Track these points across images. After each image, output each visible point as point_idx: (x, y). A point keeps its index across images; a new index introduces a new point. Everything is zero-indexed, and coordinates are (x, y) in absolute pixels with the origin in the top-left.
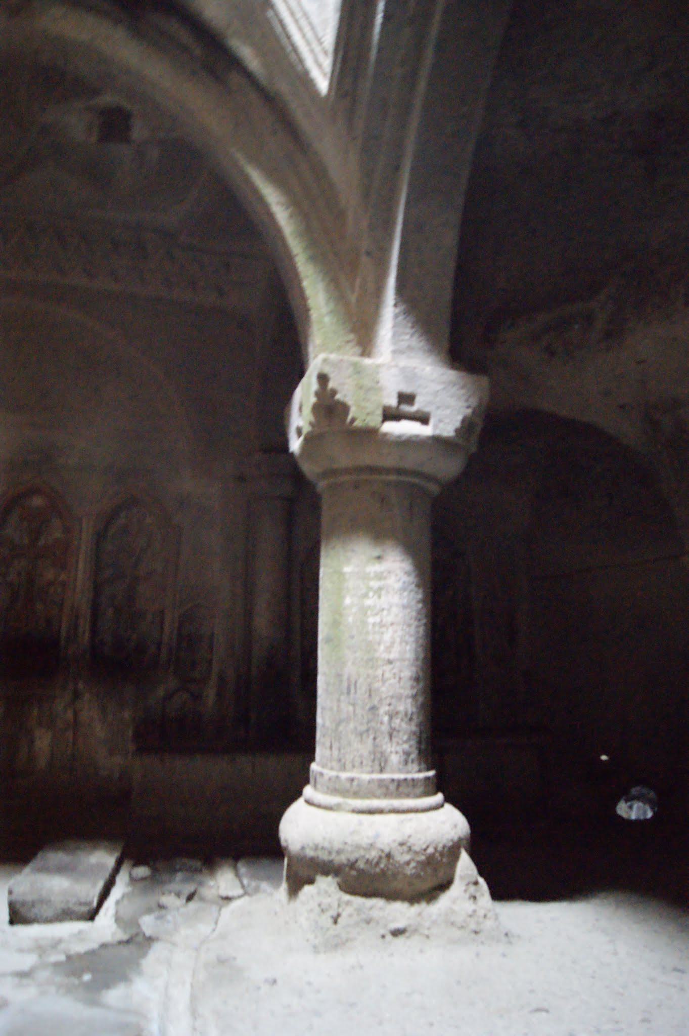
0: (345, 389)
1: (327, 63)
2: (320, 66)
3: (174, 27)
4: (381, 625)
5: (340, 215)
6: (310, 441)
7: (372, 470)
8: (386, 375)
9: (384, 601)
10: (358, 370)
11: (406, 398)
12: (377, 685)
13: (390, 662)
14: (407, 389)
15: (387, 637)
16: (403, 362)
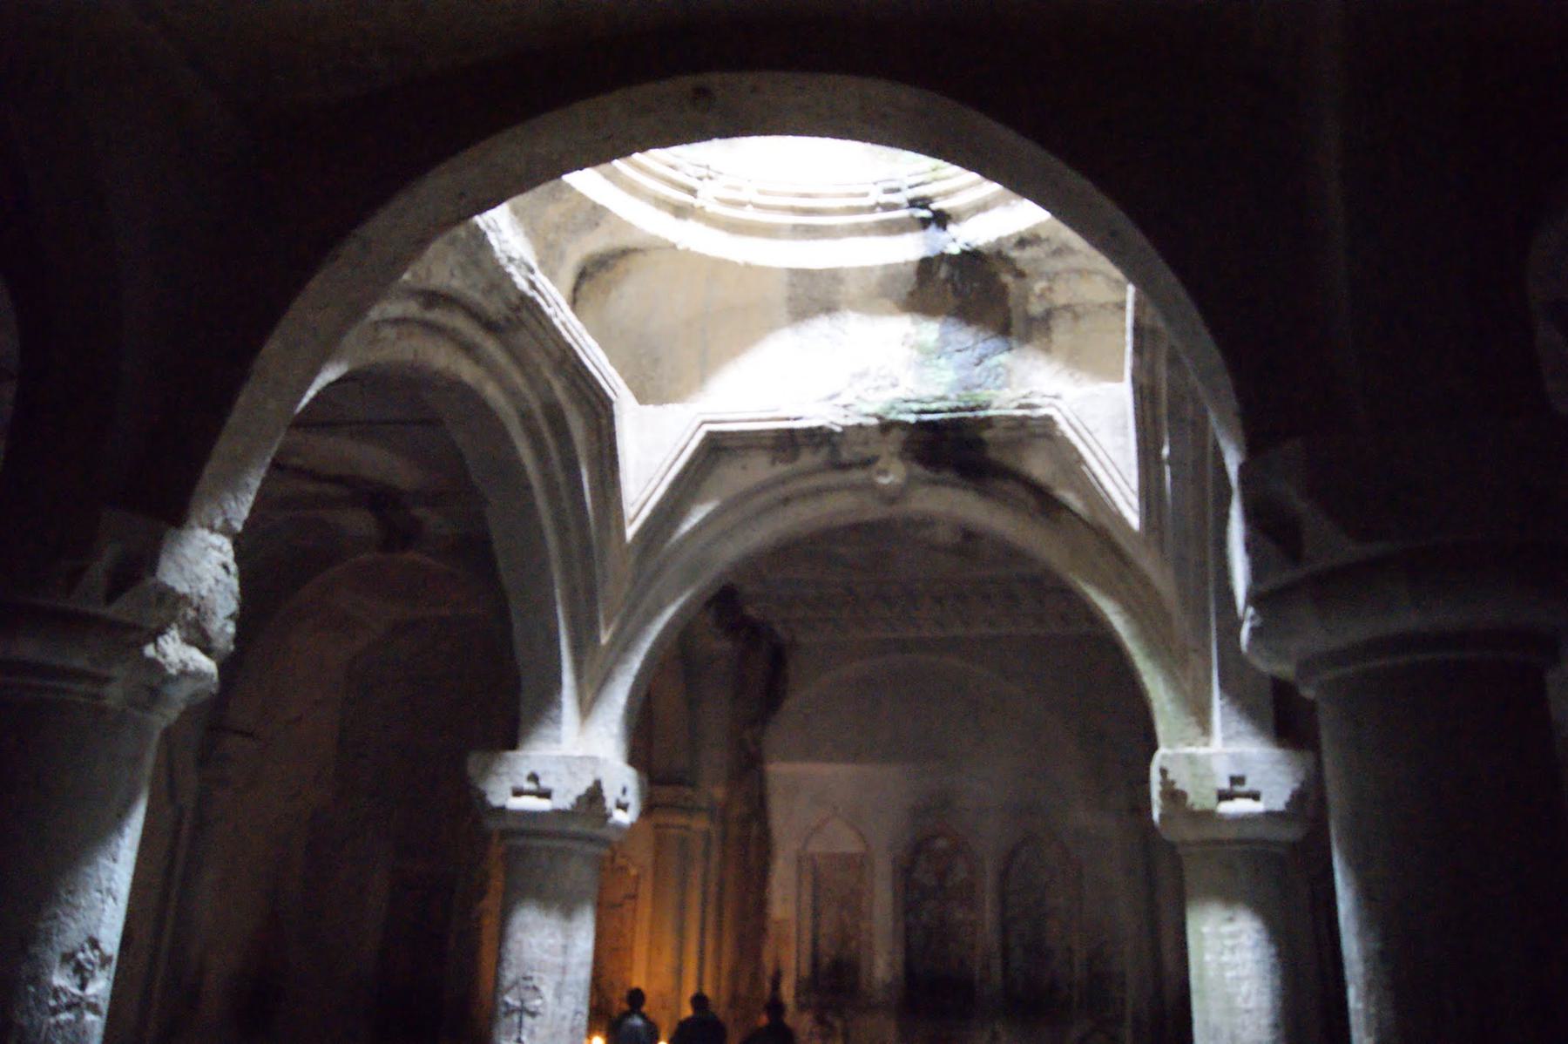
0: (1183, 781)
1: (1135, 501)
2: (1130, 504)
3: (1009, 486)
4: (1238, 979)
5: (1167, 618)
6: (1162, 816)
7: (1218, 842)
8: (1219, 760)
9: (1238, 957)
10: (1191, 759)
11: (1237, 780)
12: (1238, 1031)
13: (1248, 1011)
14: (1236, 772)
15: (1245, 988)
16: (1234, 748)
